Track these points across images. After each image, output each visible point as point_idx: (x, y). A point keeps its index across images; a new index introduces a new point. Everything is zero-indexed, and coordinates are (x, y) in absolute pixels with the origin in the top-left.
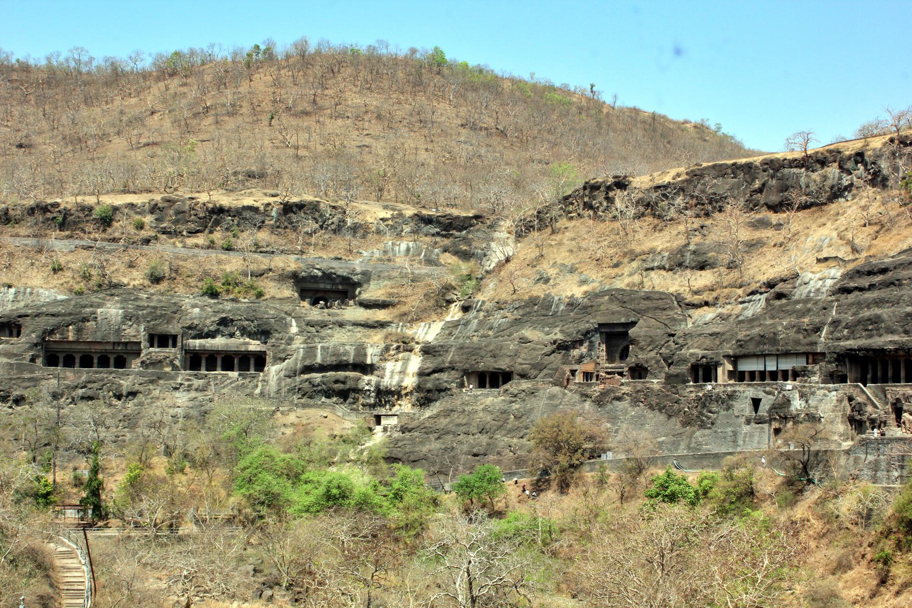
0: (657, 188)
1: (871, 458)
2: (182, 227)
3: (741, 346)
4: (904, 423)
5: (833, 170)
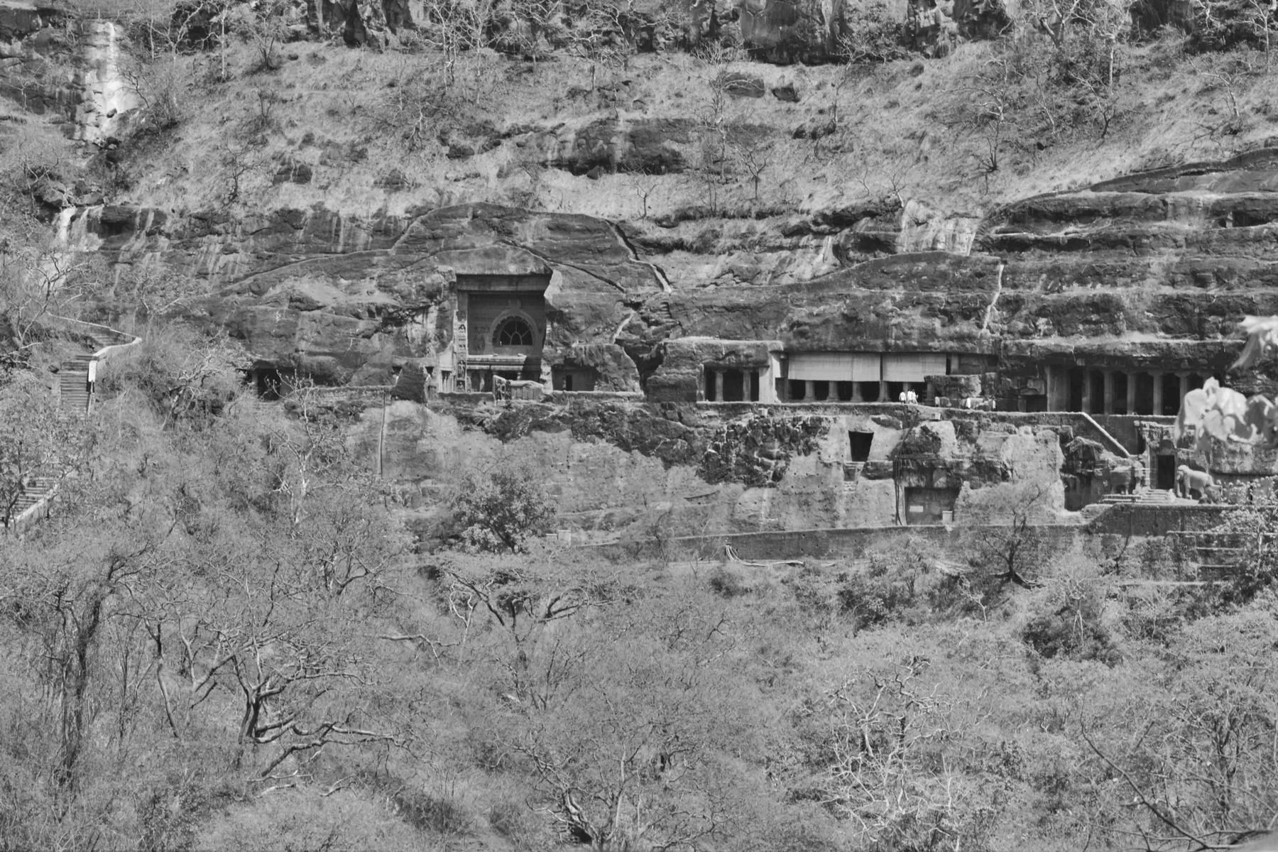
3: (802, 334)
4: (1182, 481)
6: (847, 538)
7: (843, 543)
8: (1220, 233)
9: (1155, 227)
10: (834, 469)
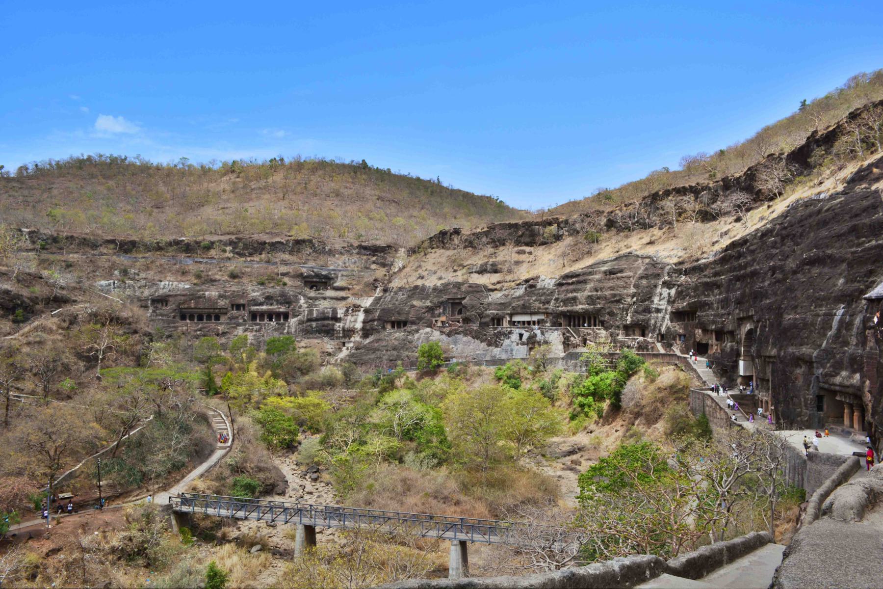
0: (474, 234)
2: (246, 253)
5: (554, 227)
9: (591, 277)
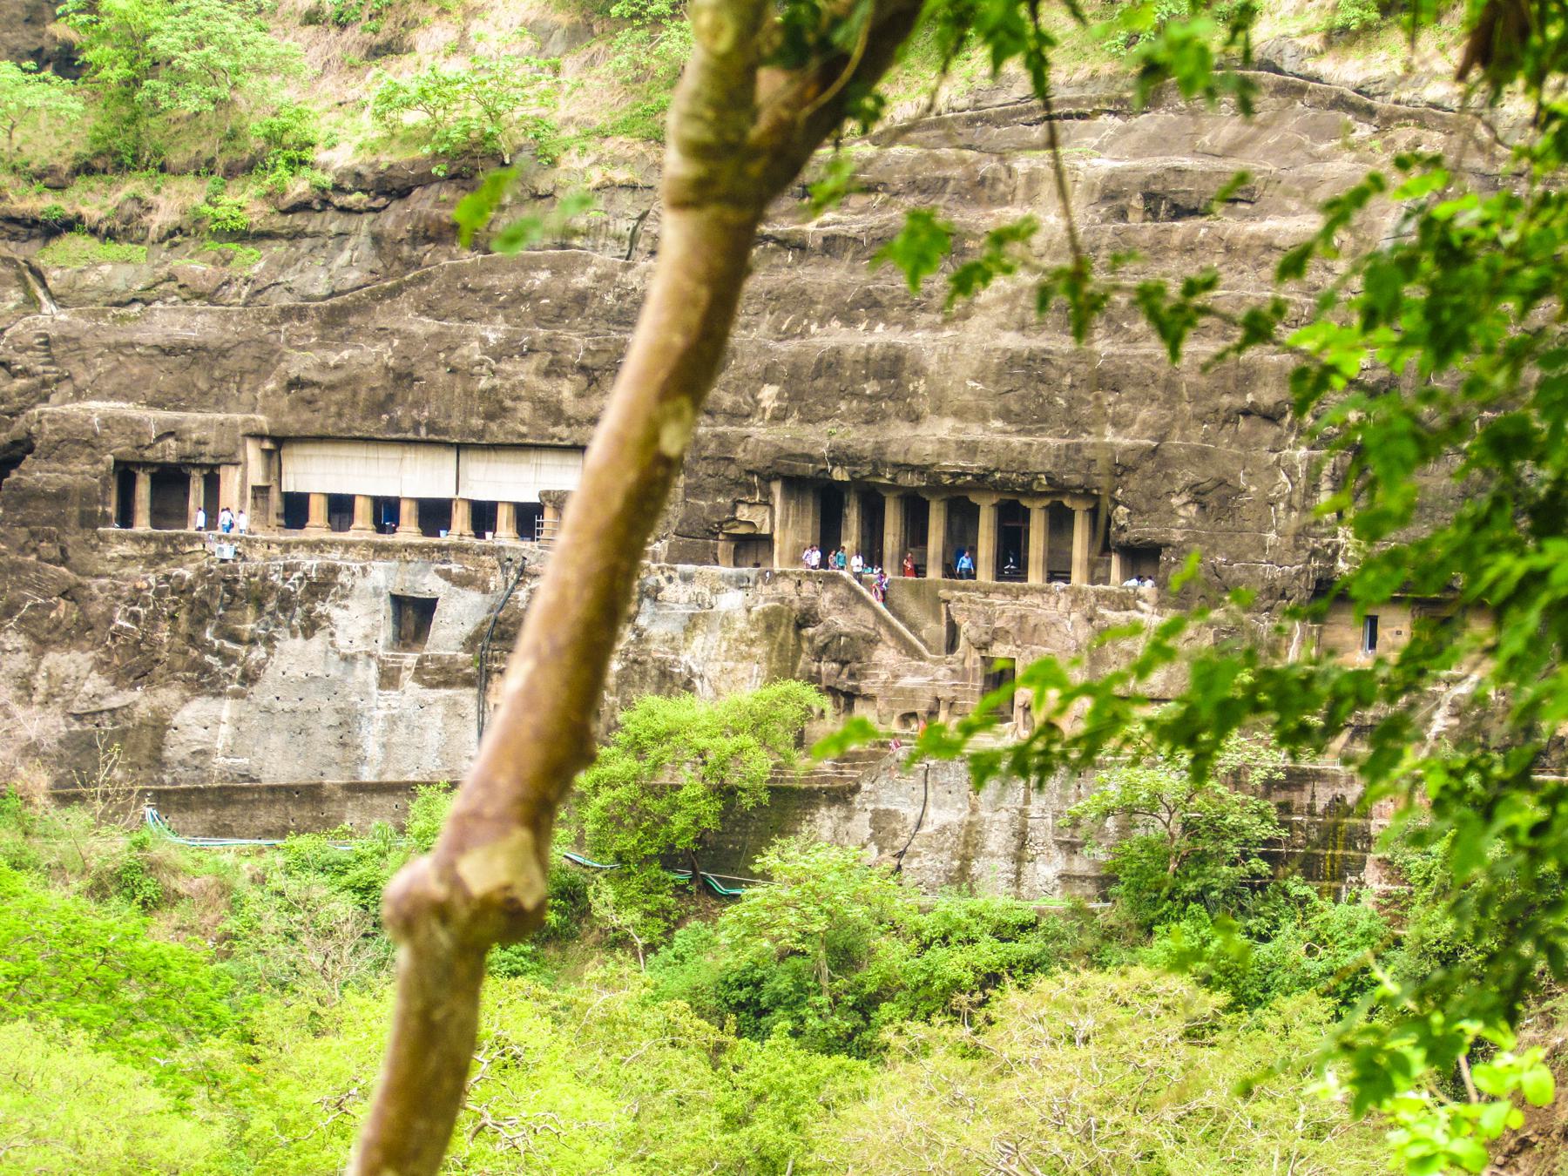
1: (937, 817)
6: (377, 800)
7: (372, 812)
8: (1116, 234)
10: (359, 665)
